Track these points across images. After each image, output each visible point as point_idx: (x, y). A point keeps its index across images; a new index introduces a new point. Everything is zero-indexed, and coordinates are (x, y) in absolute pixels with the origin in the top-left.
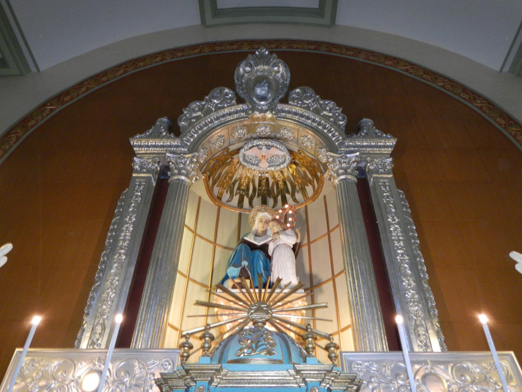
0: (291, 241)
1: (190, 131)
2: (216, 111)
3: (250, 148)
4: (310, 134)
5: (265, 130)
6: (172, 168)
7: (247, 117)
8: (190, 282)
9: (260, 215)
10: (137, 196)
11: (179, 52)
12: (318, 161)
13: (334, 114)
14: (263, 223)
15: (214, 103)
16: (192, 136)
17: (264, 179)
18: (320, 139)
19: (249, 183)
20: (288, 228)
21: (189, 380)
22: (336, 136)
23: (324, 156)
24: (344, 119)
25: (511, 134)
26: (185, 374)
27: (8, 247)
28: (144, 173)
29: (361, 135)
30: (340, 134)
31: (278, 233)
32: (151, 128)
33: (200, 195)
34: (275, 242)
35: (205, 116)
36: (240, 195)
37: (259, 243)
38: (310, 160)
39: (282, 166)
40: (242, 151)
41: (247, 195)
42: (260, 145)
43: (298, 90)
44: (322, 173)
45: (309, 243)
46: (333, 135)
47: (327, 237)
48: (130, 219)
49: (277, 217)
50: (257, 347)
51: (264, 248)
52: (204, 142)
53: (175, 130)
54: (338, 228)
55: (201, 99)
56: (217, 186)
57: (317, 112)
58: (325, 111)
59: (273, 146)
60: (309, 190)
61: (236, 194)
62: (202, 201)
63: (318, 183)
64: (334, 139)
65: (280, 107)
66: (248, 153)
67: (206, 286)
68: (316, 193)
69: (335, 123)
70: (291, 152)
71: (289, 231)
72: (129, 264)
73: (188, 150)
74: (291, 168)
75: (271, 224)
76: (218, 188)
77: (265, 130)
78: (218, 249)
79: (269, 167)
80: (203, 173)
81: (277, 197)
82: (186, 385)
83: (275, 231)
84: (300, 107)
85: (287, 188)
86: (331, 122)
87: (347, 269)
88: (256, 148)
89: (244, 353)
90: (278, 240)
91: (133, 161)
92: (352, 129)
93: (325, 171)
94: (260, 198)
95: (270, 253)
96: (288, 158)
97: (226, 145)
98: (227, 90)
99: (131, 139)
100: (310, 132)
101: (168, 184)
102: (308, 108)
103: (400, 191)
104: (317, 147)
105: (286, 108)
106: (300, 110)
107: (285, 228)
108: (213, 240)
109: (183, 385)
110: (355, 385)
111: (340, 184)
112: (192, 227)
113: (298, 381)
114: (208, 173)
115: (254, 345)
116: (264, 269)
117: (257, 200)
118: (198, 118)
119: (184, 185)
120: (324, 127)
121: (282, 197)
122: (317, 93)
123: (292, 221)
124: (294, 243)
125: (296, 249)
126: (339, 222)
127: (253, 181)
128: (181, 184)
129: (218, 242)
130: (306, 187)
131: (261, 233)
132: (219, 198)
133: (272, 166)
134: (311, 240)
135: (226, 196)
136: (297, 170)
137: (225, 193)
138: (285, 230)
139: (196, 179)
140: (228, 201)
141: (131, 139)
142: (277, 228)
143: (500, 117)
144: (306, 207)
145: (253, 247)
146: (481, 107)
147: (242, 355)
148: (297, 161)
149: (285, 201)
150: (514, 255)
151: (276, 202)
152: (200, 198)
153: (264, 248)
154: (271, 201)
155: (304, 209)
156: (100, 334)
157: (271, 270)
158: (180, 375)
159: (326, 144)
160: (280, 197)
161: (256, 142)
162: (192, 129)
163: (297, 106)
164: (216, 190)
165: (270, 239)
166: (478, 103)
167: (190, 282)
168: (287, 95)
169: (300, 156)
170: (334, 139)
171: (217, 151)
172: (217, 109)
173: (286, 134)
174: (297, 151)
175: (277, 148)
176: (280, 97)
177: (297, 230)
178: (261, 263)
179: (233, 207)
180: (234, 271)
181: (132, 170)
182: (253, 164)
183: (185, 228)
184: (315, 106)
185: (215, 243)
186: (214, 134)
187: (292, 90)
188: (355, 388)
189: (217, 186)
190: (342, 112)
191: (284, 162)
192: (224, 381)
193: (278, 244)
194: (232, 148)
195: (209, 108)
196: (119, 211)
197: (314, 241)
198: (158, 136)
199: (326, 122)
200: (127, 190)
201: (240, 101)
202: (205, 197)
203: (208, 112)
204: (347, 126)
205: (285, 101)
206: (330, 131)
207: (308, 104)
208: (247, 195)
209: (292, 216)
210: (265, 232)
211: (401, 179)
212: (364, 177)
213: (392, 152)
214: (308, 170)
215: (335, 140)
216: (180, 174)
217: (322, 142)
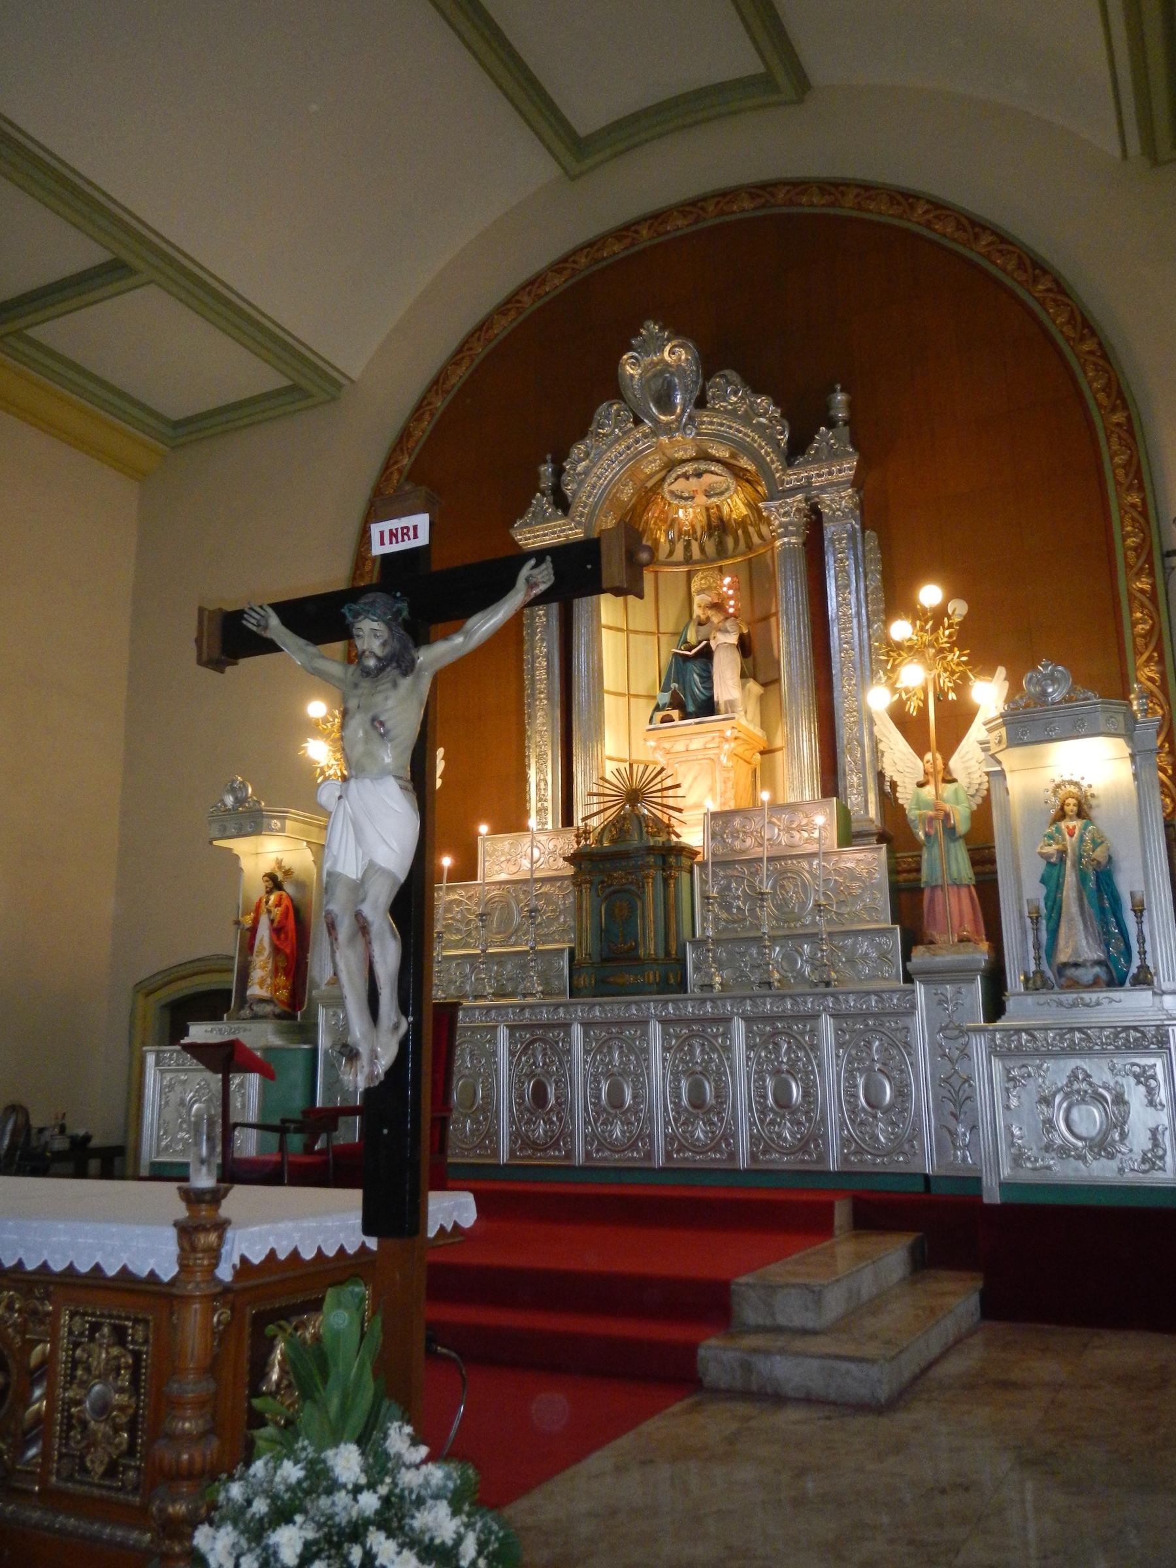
3: (676, 480)
40: (666, 486)
55: (582, 434)
57: (746, 419)
59: (707, 471)
66: (674, 487)
71: (729, 625)
72: (553, 707)
78: (664, 639)
88: (681, 480)
92: (796, 450)
102: (733, 414)
108: (654, 629)
118: (587, 472)
138: (727, 619)
140: (671, 553)
146: (1045, 298)
155: (770, 553)
160: (740, 532)
161: (680, 471)
175: (712, 473)
178: (695, 676)
180: (665, 698)
182: (686, 499)
190: (782, 415)
194: (649, 484)
205: (701, 403)
210: (708, 619)
211: (874, 512)
213: (856, 475)
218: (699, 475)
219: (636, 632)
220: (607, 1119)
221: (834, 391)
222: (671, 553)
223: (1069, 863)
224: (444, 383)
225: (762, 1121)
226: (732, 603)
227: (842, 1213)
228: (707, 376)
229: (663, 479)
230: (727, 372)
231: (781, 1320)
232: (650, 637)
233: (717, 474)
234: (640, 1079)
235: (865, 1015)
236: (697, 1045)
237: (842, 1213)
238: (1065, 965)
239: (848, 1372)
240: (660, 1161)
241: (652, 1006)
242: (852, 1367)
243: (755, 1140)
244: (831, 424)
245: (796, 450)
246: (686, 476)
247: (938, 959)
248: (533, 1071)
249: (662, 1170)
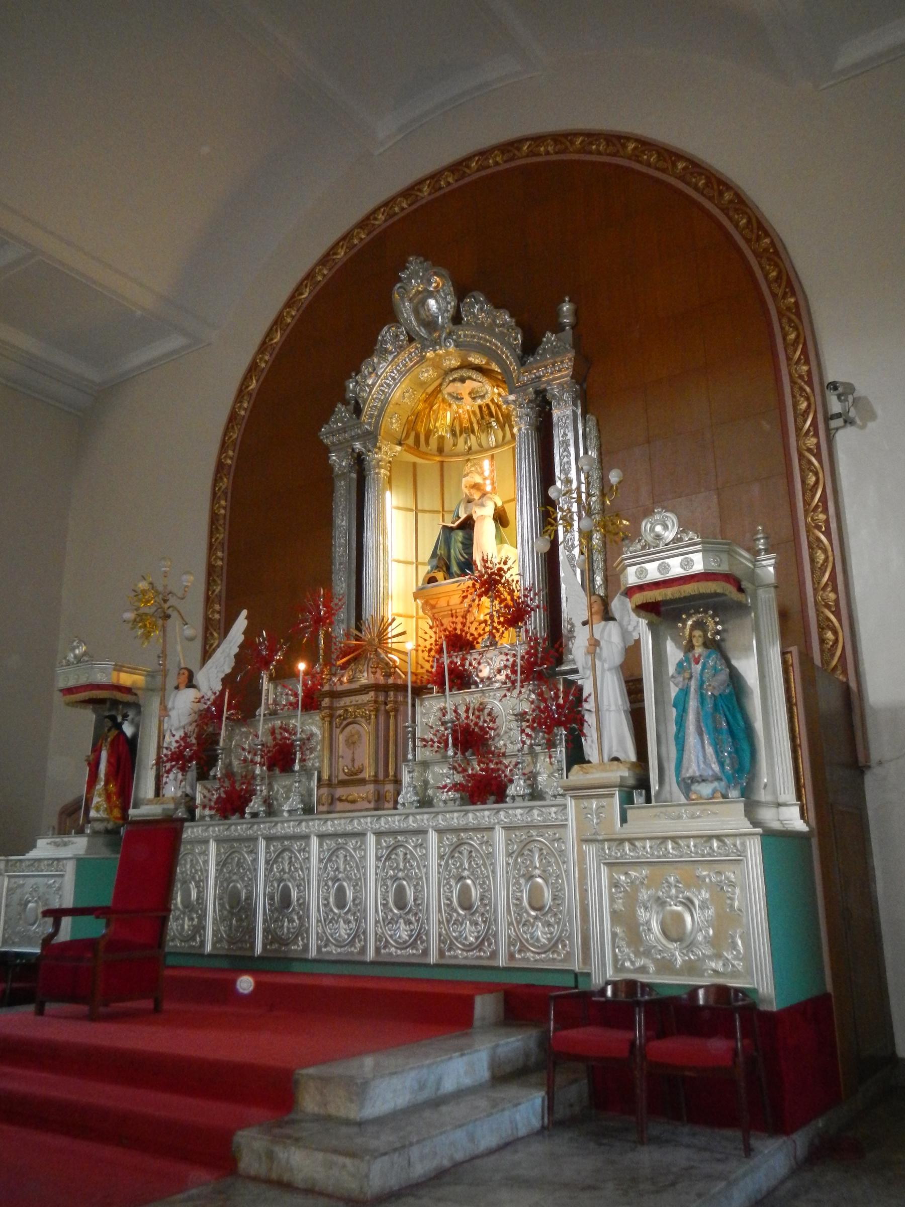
19: (470, 417)
27: (244, 613)
57: (490, 330)
59: (470, 378)
61: (461, 434)
194: (430, 390)
202: (419, 461)
218: (463, 380)
219: (424, 511)
220: (333, 919)
221: (564, 301)
222: (455, 445)
223: (692, 689)
225: (518, 923)
227: (484, 1007)
229: (441, 385)
230: (475, 293)
231: (332, 1110)
232: (435, 515)
234: (358, 884)
235: (529, 827)
236: (341, 856)
237: (484, 1007)
238: (693, 780)
239: (344, 1166)
240: (433, 959)
241: (365, 823)
242: (348, 1161)
243: (378, 938)
244: (558, 328)
247: (589, 776)
248: (336, 876)
249: (373, 963)
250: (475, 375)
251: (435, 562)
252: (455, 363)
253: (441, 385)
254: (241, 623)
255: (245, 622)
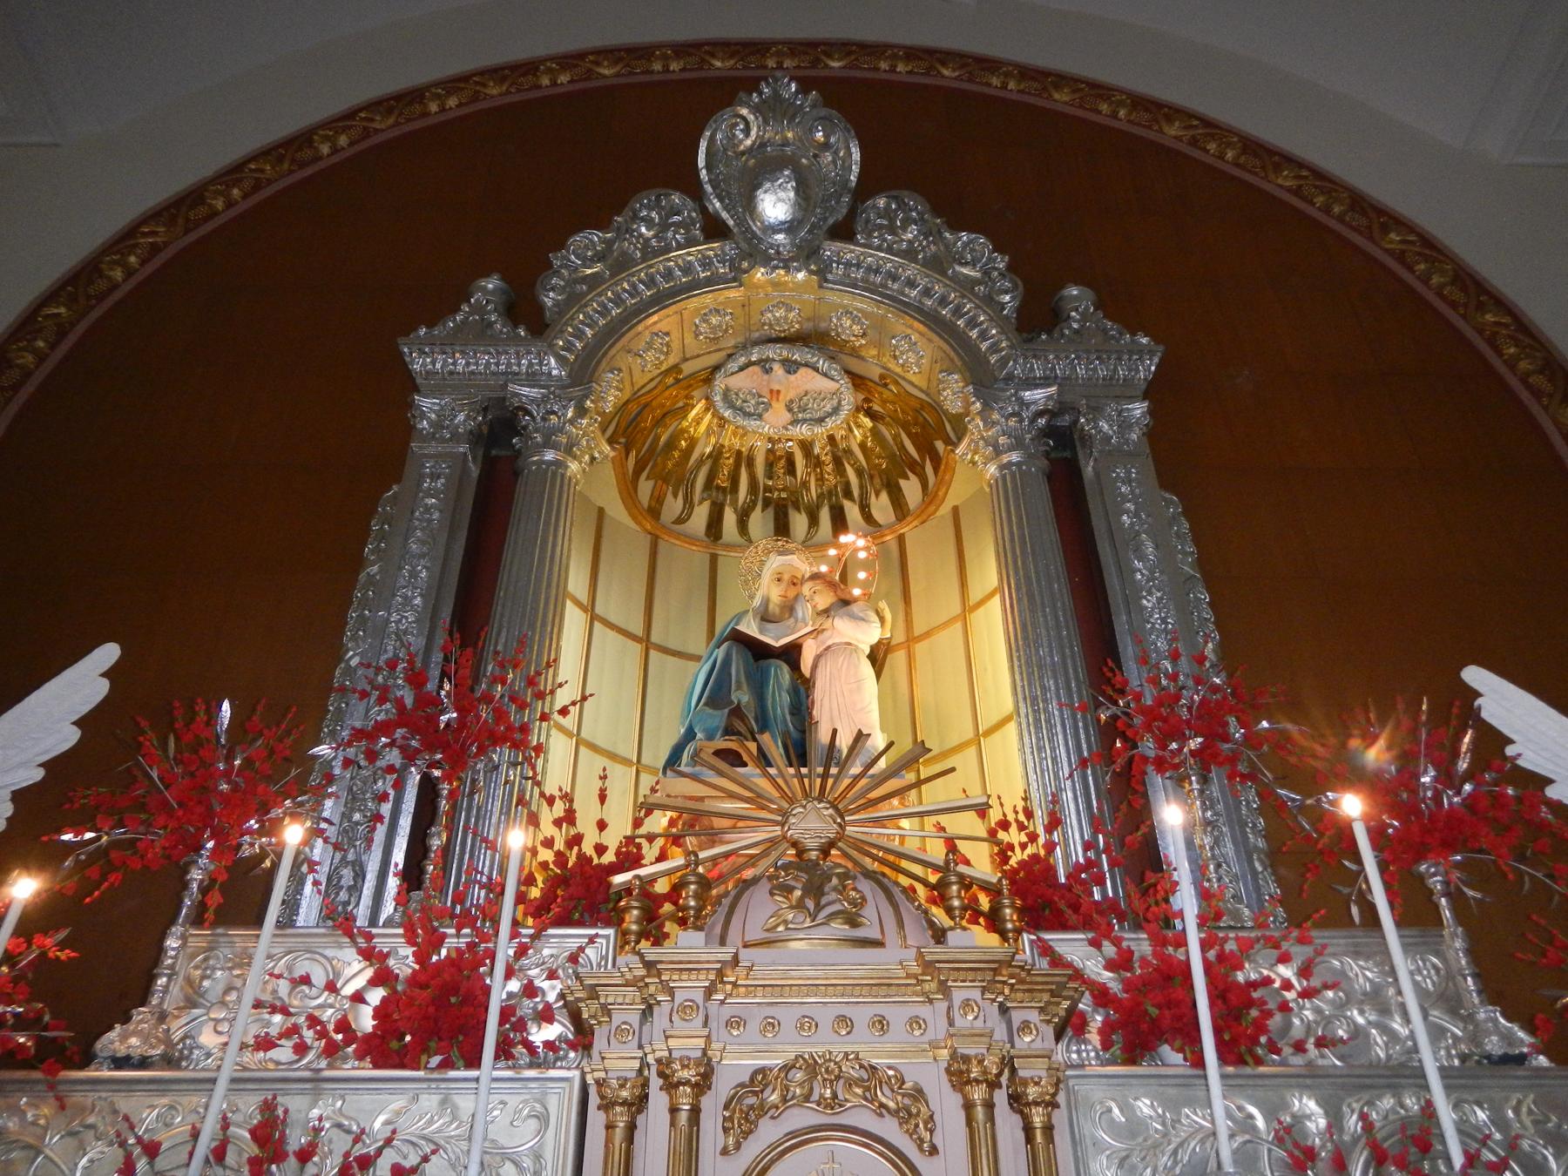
0: (871, 634)
1: (572, 318)
2: (644, 259)
3: (741, 369)
4: (916, 331)
5: (786, 318)
6: (525, 428)
7: (734, 280)
8: (582, 749)
9: (775, 562)
10: (428, 509)
11: (524, 75)
12: (936, 408)
13: (986, 273)
14: (783, 586)
15: (641, 235)
16: (579, 335)
17: (780, 458)
18: (946, 347)
20: (855, 600)
21: (652, 989)
22: (991, 338)
23: (954, 394)
24: (1015, 287)
25: (1480, 332)
26: (643, 972)
27: (108, 654)
28: (443, 440)
29: (1063, 335)
30: (1002, 332)
31: (826, 612)
32: (457, 310)
33: (600, 503)
34: (821, 637)
35: (612, 276)
36: (714, 504)
37: (775, 638)
38: (914, 403)
39: (829, 422)
41: (734, 502)
42: (768, 360)
43: (882, 202)
44: (952, 444)
45: (911, 640)
46: (983, 335)
47: (959, 625)
48: (414, 574)
49: (824, 569)
50: (819, 907)
51: (791, 654)
52: (613, 351)
53: (525, 315)
54: (997, 599)
56: (648, 478)
57: (937, 265)
58: (961, 264)
60: (911, 488)
62: (607, 522)
63: (936, 469)
64: (984, 346)
65: (830, 249)
67: (626, 762)
68: (931, 497)
69: (989, 301)
70: (858, 381)
73: (569, 376)
74: (859, 426)
75: (806, 589)
76: (651, 483)
77: (786, 318)
79: (795, 422)
80: (611, 441)
81: (818, 507)
82: (644, 1000)
83: (821, 608)
84: (890, 250)
85: (847, 485)
86: (976, 295)
87: (1023, 711)
89: (785, 922)
90: (826, 634)
91: (411, 405)
93: (960, 439)
94: (770, 512)
95: (806, 667)
96: (849, 398)
97: (672, 360)
98: (676, 198)
99: (400, 340)
100: (916, 324)
101: (516, 474)
102: (910, 254)
103: (1167, 495)
104: (938, 367)
105: (850, 252)
106: (890, 262)
107: (848, 597)
108: (640, 632)
109: (638, 1000)
110: (1066, 999)
111: (1004, 477)
112: (582, 593)
113: (927, 987)
114: (622, 440)
115: (810, 904)
116: (792, 714)
117: (760, 521)
119: (563, 475)
120: (958, 312)
121: (832, 508)
122: (937, 210)
123: (866, 580)
124: (874, 640)
125: (878, 657)
126: (1001, 580)
127: (750, 463)
128: (554, 474)
129: (655, 638)
130: (902, 482)
131: (777, 611)
132: (654, 512)
133: (804, 421)
134: (917, 632)
135: (673, 506)
136: (875, 432)
137: (670, 496)
139: (593, 459)
140: (680, 520)
141: (400, 340)
142: (824, 600)
143: (1452, 283)
144: (901, 539)
145: (758, 651)
146: (1403, 252)
147: (781, 928)
148: (876, 407)
149: (840, 523)
150: (1474, 675)
151: (814, 521)
152: (601, 511)
153: (791, 654)
154: (799, 522)
156: (350, 888)
157: (810, 714)
158: (628, 976)
159: (965, 363)
162: (578, 312)
163: (879, 249)
164: (645, 488)
165: (809, 629)
166: (1392, 242)
167: (582, 749)
168: (852, 214)
169: (886, 394)
170: (984, 346)
171: (650, 376)
172: (649, 253)
173: (848, 329)
174: (877, 379)
176: (831, 221)
177: (883, 605)
179: (691, 539)
181: (409, 430)
182: (748, 415)
183: (569, 603)
184: (933, 247)
185: (645, 641)
186: (640, 328)
187: (863, 202)
188: (1066, 1004)
189: (648, 478)
191: (836, 410)
192: (742, 990)
193: (829, 642)
194: (688, 368)
195: (624, 253)
196: (377, 550)
197: (927, 635)
198: (480, 335)
199: (963, 296)
200: (395, 488)
201: (715, 229)
202: (617, 511)
203: (622, 265)
204: (1020, 311)
205: (844, 231)
206: (972, 323)
207: (910, 242)
208: (734, 502)
209: (865, 565)
212: (1067, 454)
214: (909, 435)
215: (988, 349)
216: (548, 444)
217: (952, 354)
218: (791, 367)
222: (680, 520)
224: (300, 149)
226: (862, 575)
228: (864, 190)
229: (716, 368)
232: (630, 642)
233: (825, 375)
245: (1037, 319)
246: (765, 365)
250: (823, 364)
251: (719, 718)
252: (791, 320)
253: (716, 368)
254: (83, 684)
255: (103, 687)
